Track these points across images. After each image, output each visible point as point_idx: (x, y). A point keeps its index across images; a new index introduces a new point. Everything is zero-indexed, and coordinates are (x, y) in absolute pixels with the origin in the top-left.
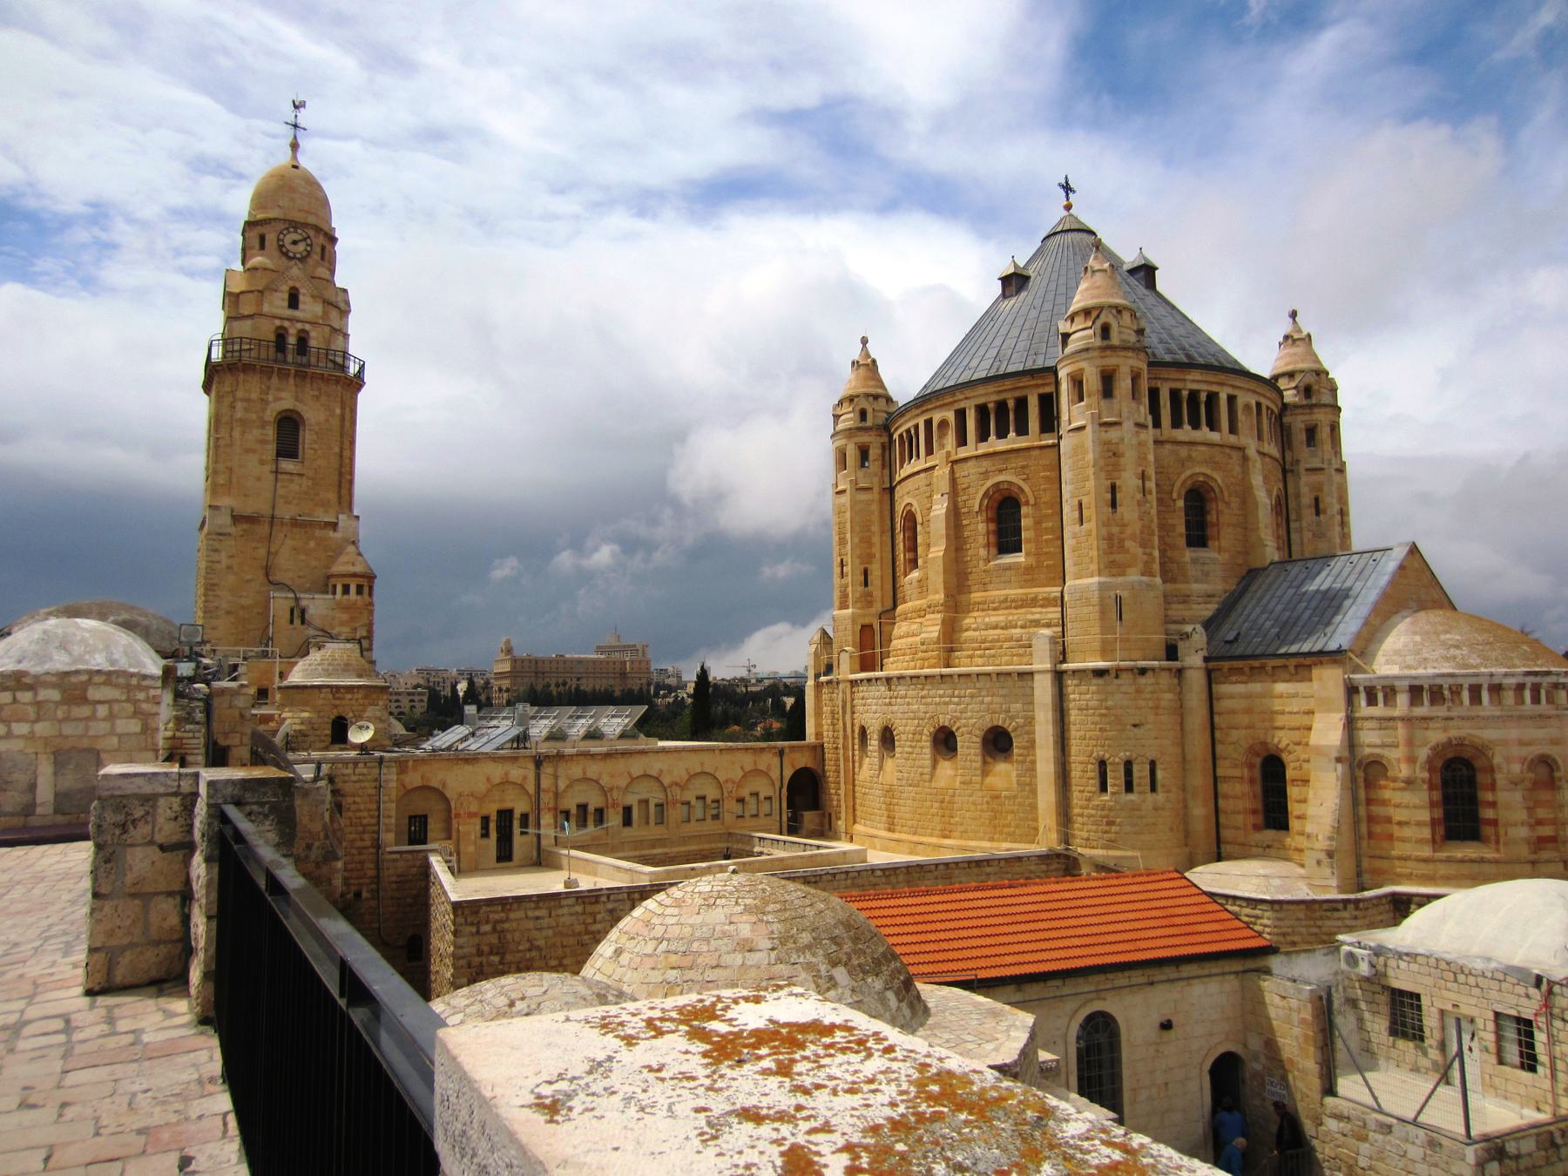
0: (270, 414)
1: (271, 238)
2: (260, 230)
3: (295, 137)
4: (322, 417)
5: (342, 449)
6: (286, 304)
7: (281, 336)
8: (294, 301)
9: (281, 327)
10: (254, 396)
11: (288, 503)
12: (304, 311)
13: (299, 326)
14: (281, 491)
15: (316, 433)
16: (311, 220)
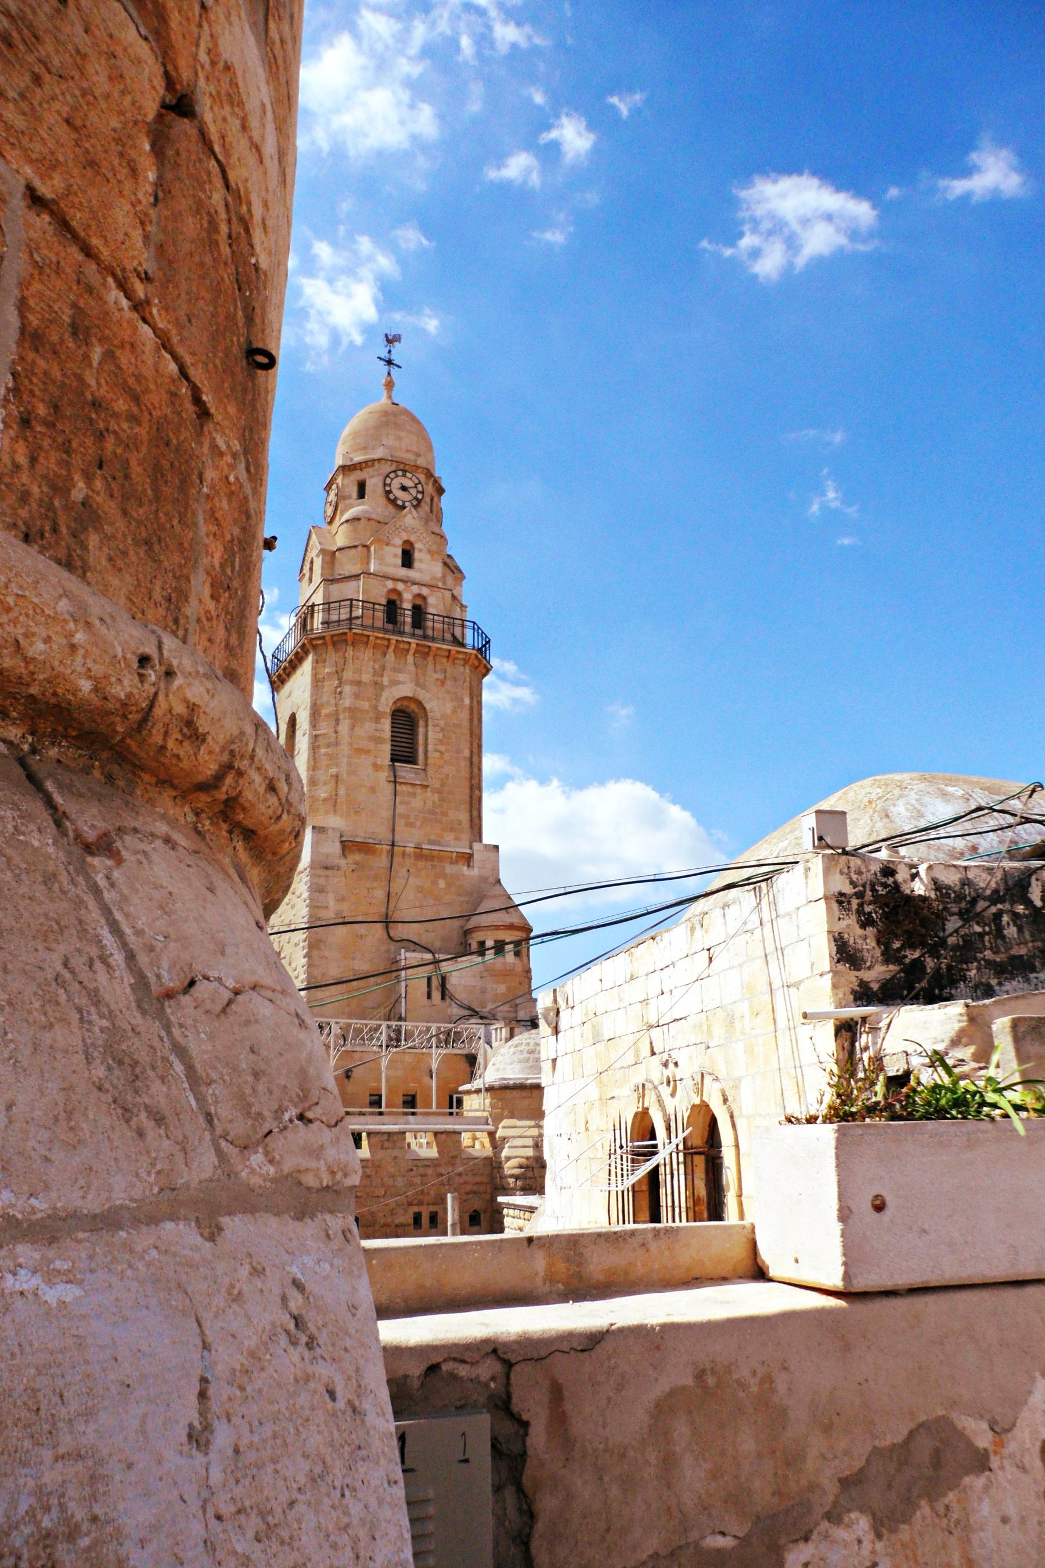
0: (386, 704)
1: (374, 484)
2: (358, 475)
3: (389, 374)
4: (448, 707)
5: (472, 752)
6: (399, 561)
7: (392, 608)
8: (407, 559)
9: (394, 591)
10: (366, 677)
11: (410, 825)
12: (421, 571)
13: (415, 589)
14: (400, 809)
15: (442, 730)
16: (421, 462)
